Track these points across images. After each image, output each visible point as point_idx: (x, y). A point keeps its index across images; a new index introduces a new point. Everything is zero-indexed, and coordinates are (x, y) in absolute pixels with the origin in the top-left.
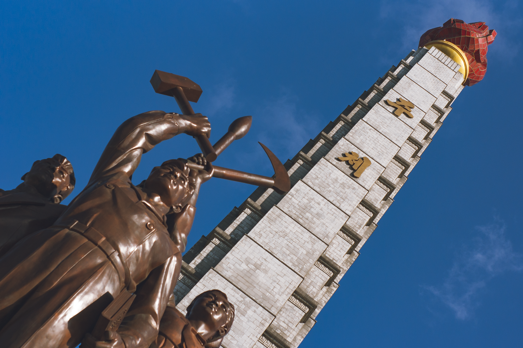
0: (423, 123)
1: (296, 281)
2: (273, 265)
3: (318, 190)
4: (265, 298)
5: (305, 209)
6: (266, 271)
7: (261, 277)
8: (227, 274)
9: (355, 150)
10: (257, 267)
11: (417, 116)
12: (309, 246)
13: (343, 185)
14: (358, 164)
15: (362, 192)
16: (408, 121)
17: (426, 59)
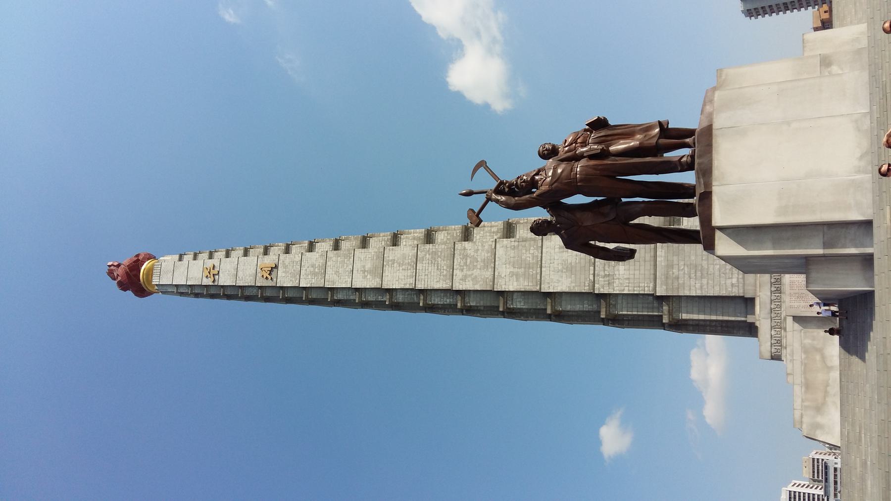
0: (211, 256)
1: (359, 252)
2: (358, 265)
3: (298, 277)
4: (378, 257)
5: (314, 274)
6: (364, 267)
7: (368, 266)
8: (378, 280)
9: (259, 275)
10: (364, 271)
11: (210, 263)
12: (334, 259)
13: (286, 267)
14: (266, 269)
15: (283, 256)
16: (217, 265)
17: (165, 281)
